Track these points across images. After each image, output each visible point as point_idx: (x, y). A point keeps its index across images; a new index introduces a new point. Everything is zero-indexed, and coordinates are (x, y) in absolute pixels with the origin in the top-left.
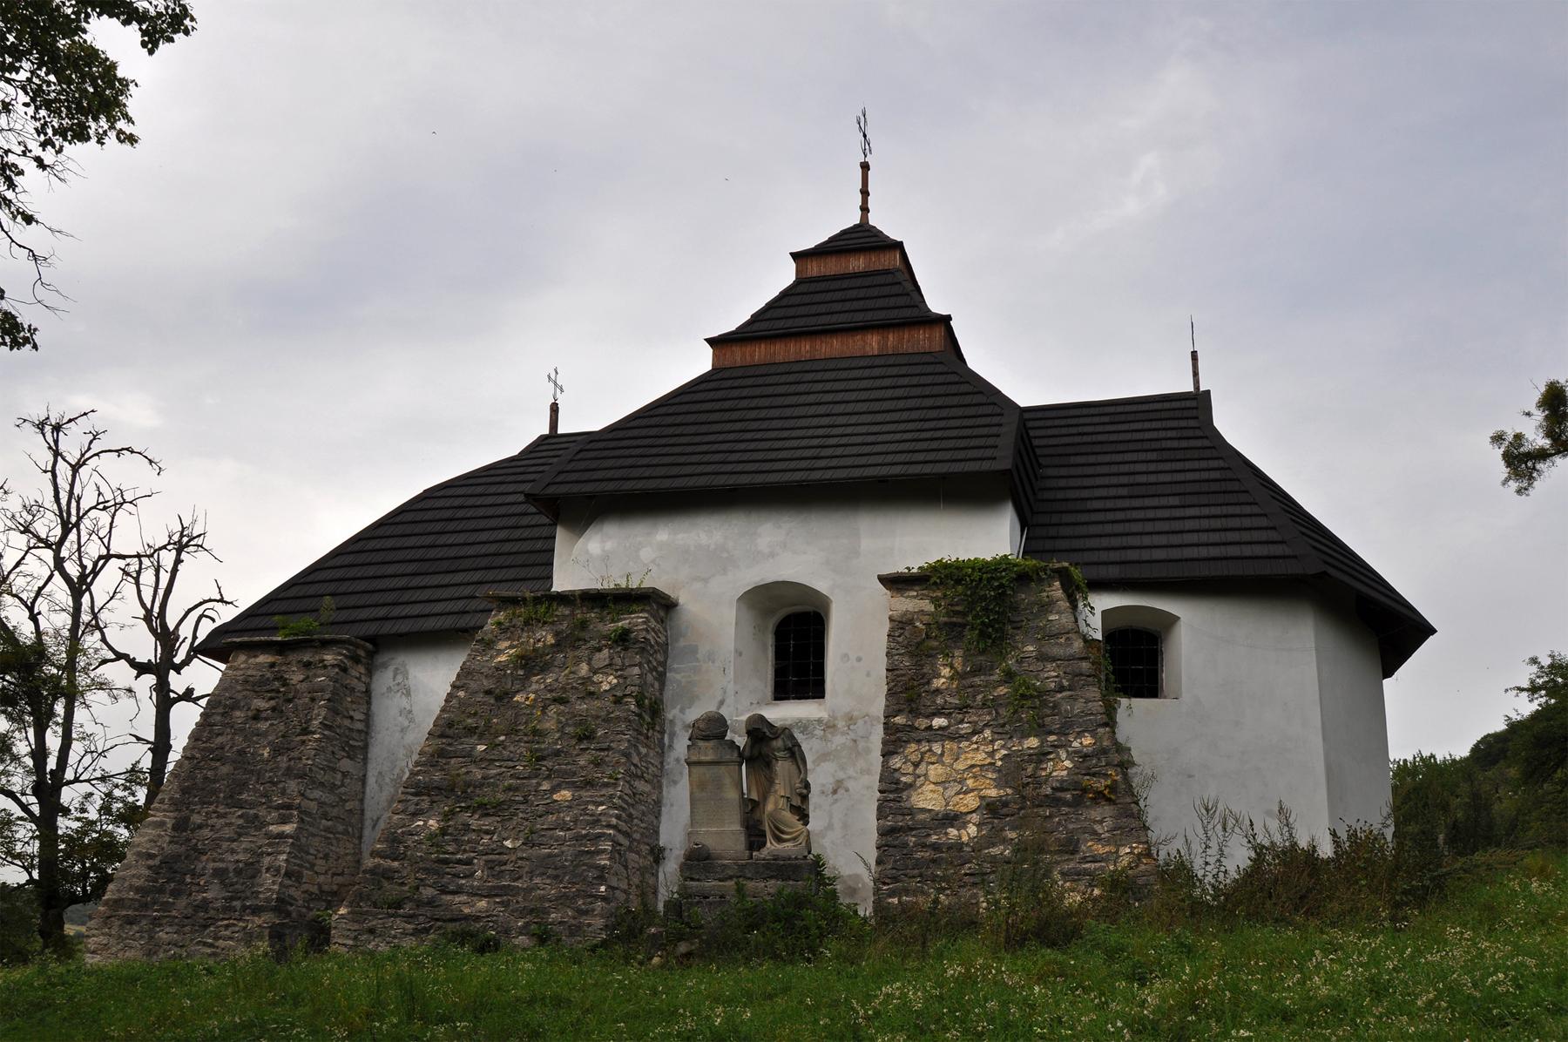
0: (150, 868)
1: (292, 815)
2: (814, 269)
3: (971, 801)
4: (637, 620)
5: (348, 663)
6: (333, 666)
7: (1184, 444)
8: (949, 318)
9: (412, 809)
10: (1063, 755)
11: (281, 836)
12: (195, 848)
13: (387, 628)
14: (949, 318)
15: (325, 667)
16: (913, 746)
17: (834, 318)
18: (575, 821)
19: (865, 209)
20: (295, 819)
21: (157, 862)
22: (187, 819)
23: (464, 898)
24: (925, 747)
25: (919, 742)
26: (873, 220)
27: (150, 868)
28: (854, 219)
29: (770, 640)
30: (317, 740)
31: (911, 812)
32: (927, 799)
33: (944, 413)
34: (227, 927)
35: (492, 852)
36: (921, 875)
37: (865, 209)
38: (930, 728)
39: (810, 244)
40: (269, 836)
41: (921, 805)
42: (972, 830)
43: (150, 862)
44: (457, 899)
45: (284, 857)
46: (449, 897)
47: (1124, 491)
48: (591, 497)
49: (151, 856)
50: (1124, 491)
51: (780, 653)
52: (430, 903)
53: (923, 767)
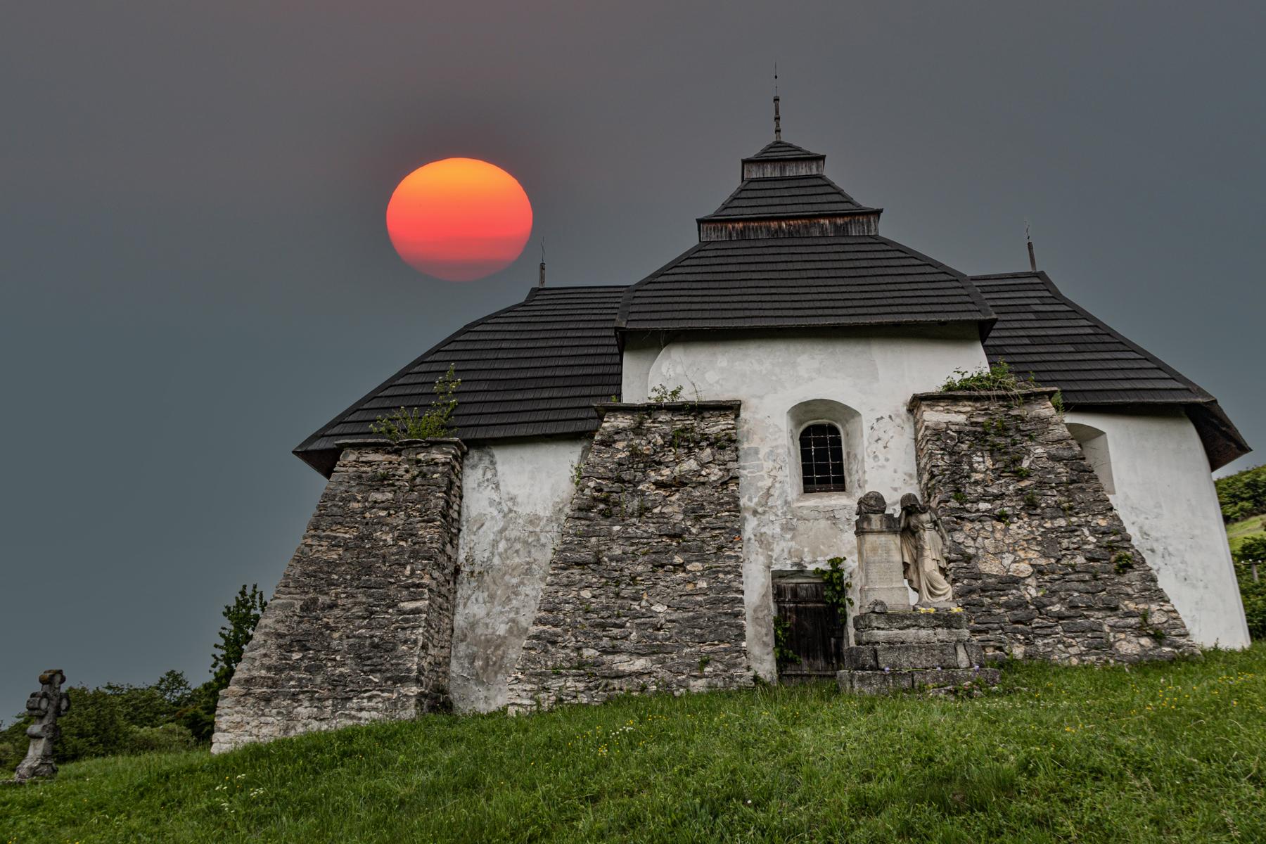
0: (280, 647)
1: (423, 593)
2: (755, 173)
3: (1024, 569)
4: (717, 426)
5: (454, 463)
6: (444, 464)
9: (565, 581)
10: (1086, 532)
11: (416, 611)
12: (327, 626)
13: (480, 434)
15: (436, 464)
16: (968, 526)
17: (790, 208)
18: (710, 588)
19: (778, 131)
20: (426, 596)
21: (287, 640)
22: (315, 601)
23: (624, 657)
24: (978, 525)
25: (972, 521)
26: (785, 138)
27: (280, 647)
28: (772, 138)
30: (439, 527)
31: (978, 576)
32: (990, 567)
34: (370, 698)
35: (643, 616)
36: (1002, 628)
37: (778, 131)
38: (978, 510)
39: (751, 155)
40: (401, 612)
41: (987, 570)
42: (1033, 592)
43: (280, 641)
44: (617, 658)
45: (421, 630)
46: (610, 657)
49: (280, 636)
51: (805, 455)
52: (596, 664)
53: (980, 539)
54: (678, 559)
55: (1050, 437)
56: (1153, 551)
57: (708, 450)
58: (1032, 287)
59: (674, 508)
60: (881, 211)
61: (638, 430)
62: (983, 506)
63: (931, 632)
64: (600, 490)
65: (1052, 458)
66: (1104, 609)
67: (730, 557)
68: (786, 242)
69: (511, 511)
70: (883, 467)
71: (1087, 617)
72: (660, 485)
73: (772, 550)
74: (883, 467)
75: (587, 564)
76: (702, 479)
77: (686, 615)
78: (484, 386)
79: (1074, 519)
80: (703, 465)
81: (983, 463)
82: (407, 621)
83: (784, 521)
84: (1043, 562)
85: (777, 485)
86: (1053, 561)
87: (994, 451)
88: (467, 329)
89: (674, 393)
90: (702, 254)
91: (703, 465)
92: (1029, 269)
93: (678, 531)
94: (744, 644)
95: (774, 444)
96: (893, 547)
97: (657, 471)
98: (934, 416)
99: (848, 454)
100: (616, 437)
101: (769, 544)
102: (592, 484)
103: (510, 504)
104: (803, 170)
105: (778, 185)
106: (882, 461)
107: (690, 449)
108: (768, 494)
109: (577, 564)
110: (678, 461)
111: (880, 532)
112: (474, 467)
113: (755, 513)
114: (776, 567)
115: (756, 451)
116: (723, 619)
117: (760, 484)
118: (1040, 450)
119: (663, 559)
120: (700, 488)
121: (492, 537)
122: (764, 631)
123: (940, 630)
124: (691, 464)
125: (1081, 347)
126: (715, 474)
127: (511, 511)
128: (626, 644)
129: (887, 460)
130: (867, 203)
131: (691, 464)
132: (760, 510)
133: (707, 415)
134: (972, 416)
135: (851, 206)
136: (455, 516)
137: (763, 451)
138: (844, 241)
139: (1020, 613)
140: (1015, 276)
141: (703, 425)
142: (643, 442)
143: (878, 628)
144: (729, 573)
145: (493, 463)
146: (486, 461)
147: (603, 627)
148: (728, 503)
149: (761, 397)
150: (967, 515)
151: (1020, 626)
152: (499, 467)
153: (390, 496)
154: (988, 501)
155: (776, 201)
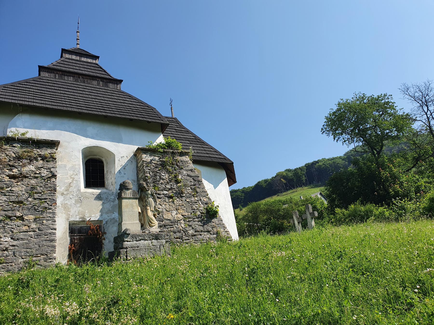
4: (46, 152)
32: (167, 216)
48: (21, 105)
54: (18, 214)
55: (187, 168)
57: (41, 162)
59: (19, 188)
62: (165, 192)
63: (150, 242)
65: (188, 175)
66: (206, 231)
67: (50, 213)
70: (123, 177)
71: (201, 235)
73: (70, 212)
74: (123, 177)
76: (37, 175)
79: (196, 198)
80: (39, 168)
81: (166, 176)
83: (77, 198)
84: (186, 214)
85: (74, 182)
86: (190, 214)
89: (23, 134)
92: (170, 116)
94: (55, 255)
95: (74, 163)
96: (135, 205)
97: (11, 170)
99: (107, 171)
101: (69, 209)
104: (90, 60)
106: (123, 174)
107: (31, 161)
108: (70, 185)
110: (24, 166)
111: (130, 198)
113: (62, 194)
114: (72, 219)
115: (65, 166)
116: (44, 243)
117: (66, 181)
118: (185, 172)
119: (10, 213)
120: (35, 180)
122: (63, 250)
123: (154, 240)
124: (32, 168)
129: (125, 174)
131: (32, 168)
132: (65, 193)
134: (160, 158)
137: (69, 166)
139: (178, 235)
141: (38, 150)
142: (3, 155)
143: (127, 241)
144: (48, 220)
148: (50, 187)
149: (69, 142)
151: (178, 240)
154: (167, 191)
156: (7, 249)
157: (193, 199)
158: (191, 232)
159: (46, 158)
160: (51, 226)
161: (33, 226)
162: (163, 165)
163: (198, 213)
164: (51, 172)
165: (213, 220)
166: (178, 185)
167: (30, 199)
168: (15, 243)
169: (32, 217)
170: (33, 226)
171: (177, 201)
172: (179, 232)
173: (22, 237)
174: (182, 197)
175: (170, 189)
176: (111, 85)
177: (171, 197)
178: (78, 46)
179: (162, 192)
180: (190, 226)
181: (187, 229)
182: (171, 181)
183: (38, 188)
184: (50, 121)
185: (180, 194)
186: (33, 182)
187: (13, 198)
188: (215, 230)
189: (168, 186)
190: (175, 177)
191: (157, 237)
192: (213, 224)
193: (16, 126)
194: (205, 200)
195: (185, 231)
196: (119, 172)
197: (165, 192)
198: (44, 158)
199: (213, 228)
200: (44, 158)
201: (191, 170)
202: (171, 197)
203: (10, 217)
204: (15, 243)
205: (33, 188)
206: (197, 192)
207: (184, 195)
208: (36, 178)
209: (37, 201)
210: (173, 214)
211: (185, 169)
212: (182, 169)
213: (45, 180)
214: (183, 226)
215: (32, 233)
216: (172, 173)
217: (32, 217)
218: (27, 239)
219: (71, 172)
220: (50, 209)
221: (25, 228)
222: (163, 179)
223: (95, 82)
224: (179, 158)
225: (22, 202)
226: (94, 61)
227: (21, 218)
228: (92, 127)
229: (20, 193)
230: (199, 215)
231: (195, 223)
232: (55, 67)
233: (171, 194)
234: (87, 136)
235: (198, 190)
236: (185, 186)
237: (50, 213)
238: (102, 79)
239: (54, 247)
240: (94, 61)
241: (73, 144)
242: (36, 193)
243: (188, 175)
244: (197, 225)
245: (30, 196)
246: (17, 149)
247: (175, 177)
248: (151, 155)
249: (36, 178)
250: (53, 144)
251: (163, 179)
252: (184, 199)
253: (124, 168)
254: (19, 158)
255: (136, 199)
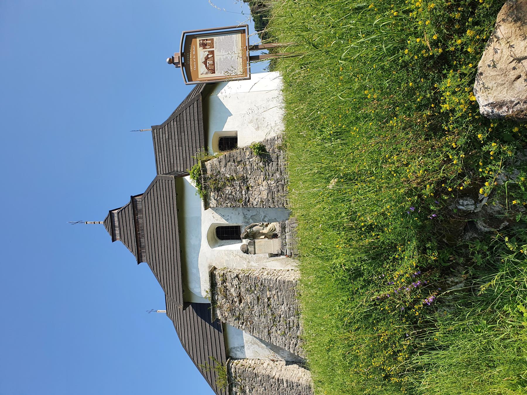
7: (167, 133)
8: (154, 128)
10: (251, 160)
14: (154, 128)
17: (132, 228)
29: (224, 241)
33: (159, 196)
39: (111, 238)
47: (181, 148)
50: (181, 148)
54: (266, 300)
55: (218, 167)
56: (257, 119)
58: (158, 134)
59: (248, 298)
60: (131, 196)
61: (220, 308)
62: (243, 192)
64: (243, 323)
65: (225, 166)
67: (265, 281)
68: (146, 233)
69: (251, 342)
70: (231, 217)
72: (240, 302)
74: (231, 217)
75: (269, 331)
76: (238, 287)
77: (285, 300)
78: (206, 347)
79: (247, 163)
80: (233, 286)
81: (228, 189)
82: (290, 386)
84: (262, 177)
86: (262, 173)
87: (224, 185)
88: (184, 347)
89: (207, 292)
90: (152, 264)
91: (233, 286)
93: (256, 298)
98: (213, 203)
100: (224, 315)
102: (241, 326)
103: (248, 342)
104: (116, 219)
105: (122, 229)
106: (229, 218)
107: (227, 289)
109: (269, 334)
110: (231, 294)
111: (255, 248)
112: (236, 354)
113: (249, 262)
115: (227, 261)
117: (238, 260)
119: (266, 305)
121: (260, 349)
124: (232, 290)
125: (182, 130)
126: (235, 282)
127: (251, 342)
128: (295, 321)
129: (228, 216)
130: (129, 200)
131: (232, 290)
133: (214, 282)
135: (130, 206)
136: (253, 362)
138: (144, 210)
139: (280, 188)
140: (154, 138)
145: (234, 348)
146: (234, 350)
147: (290, 328)
148: (246, 279)
149: (207, 258)
150: (247, 199)
152: (236, 346)
153: (247, 387)
155: (129, 232)
156: (290, 308)
157: (248, 167)
158: (278, 175)
159: (224, 280)
160: (274, 282)
161: (274, 292)
162: (218, 190)
163: (261, 164)
164: (234, 278)
165: (268, 150)
166: (235, 178)
167: (256, 292)
168: (285, 303)
169: (268, 293)
170: (274, 292)
171: (251, 182)
172: (278, 187)
173: (281, 299)
174: (247, 178)
175: (240, 187)
176: (139, 207)
177: (248, 188)
178: (102, 222)
179: (244, 196)
180: (273, 175)
181: (276, 179)
182: (233, 186)
183: (247, 287)
184: (192, 270)
185: (244, 180)
186: (243, 290)
187: (256, 302)
188: (276, 150)
189: (238, 188)
190: (228, 180)
191: (283, 228)
192: (271, 151)
193: (200, 292)
194: (248, 153)
195: (277, 181)
196: (227, 220)
197: (243, 192)
198: (224, 281)
199: (274, 152)
200: (224, 281)
201: (220, 162)
202: (248, 188)
203: (268, 305)
204: (285, 303)
205: (247, 290)
206: (241, 161)
207: (245, 175)
208: (240, 288)
209: (257, 289)
210: (263, 189)
211: (219, 169)
212: (219, 172)
213: (241, 283)
214: (273, 182)
215: (279, 294)
216: (225, 183)
217: (268, 293)
218: (283, 297)
219: (231, 256)
220: (262, 281)
221: (276, 297)
222: (232, 192)
223: (140, 221)
224: (209, 172)
225: (258, 297)
226: (116, 215)
227: (269, 299)
228: (191, 241)
229: (251, 298)
230: (263, 164)
231: (270, 170)
232: (134, 250)
233: (245, 188)
234: (200, 245)
235: (239, 159)
236: (236, 172)
237: (265, 281)
238: (135, 214)
239: (288, 282)
240: (116, 215)
241: (208, 257)
242: (251, 288)
243: (225, 166)
244: (272, 167)
245: (253, 292)
246: (219, 298)
247: (228, 180)
248: (210, 200)
249: (240, 288)
250: (212, 276)
251: (232, 192)
252: (249, 176)
253: (223, 216)
254: (226, 297)
255: (254, 242)
